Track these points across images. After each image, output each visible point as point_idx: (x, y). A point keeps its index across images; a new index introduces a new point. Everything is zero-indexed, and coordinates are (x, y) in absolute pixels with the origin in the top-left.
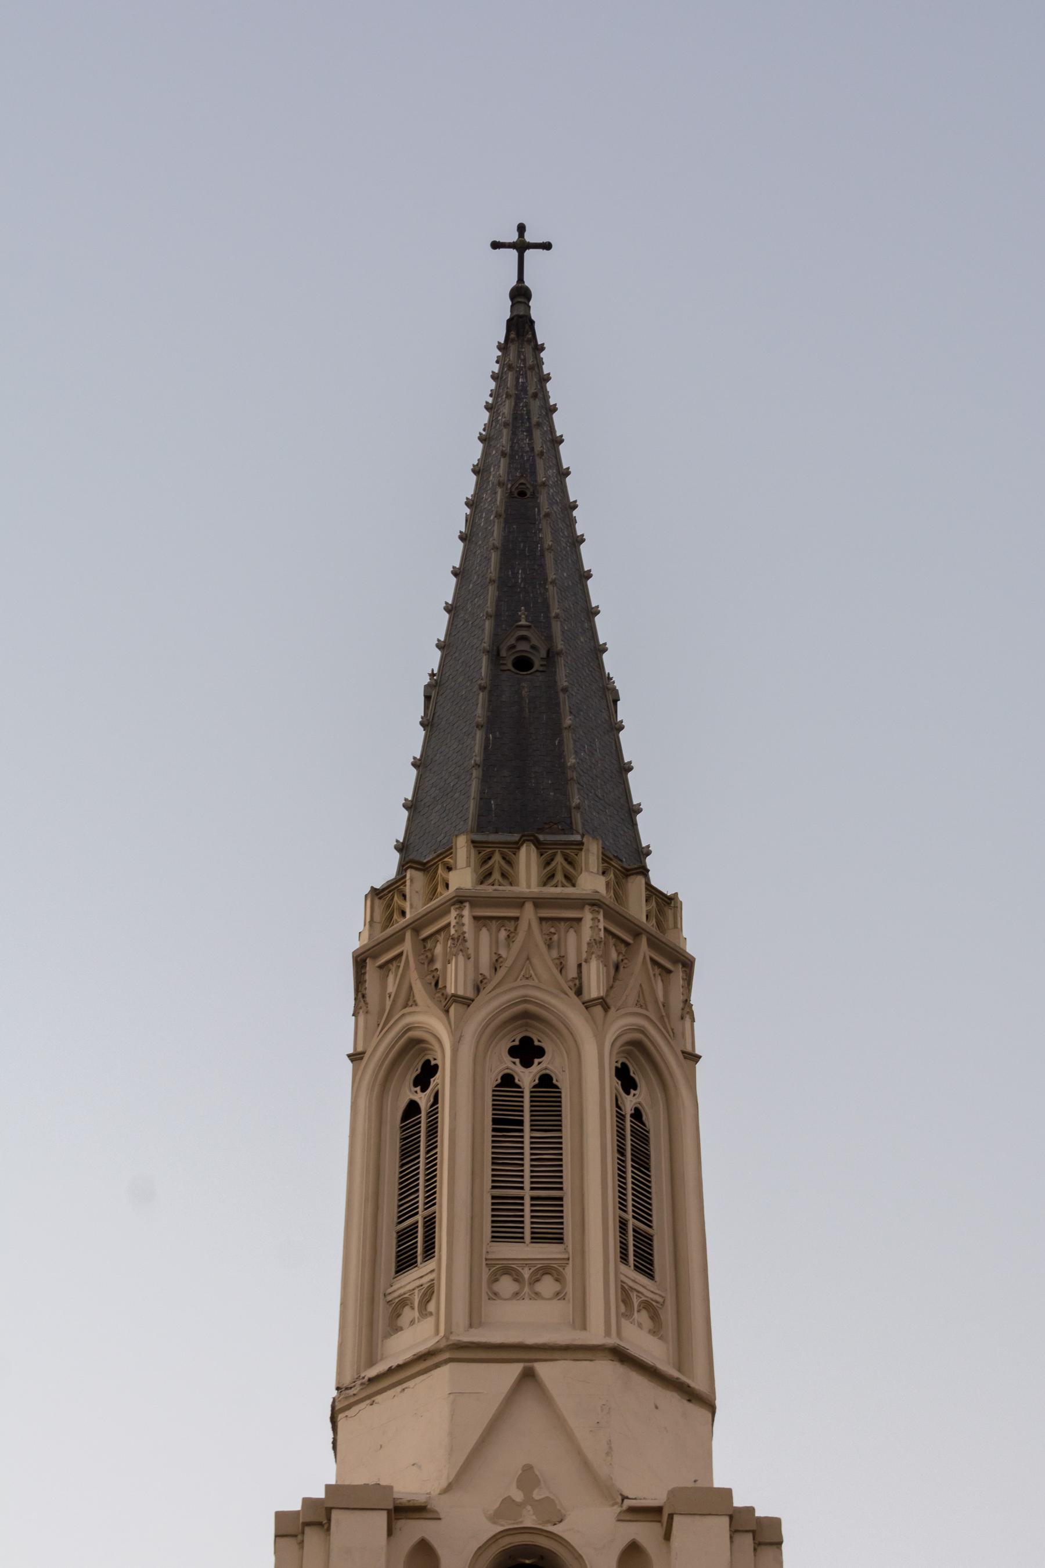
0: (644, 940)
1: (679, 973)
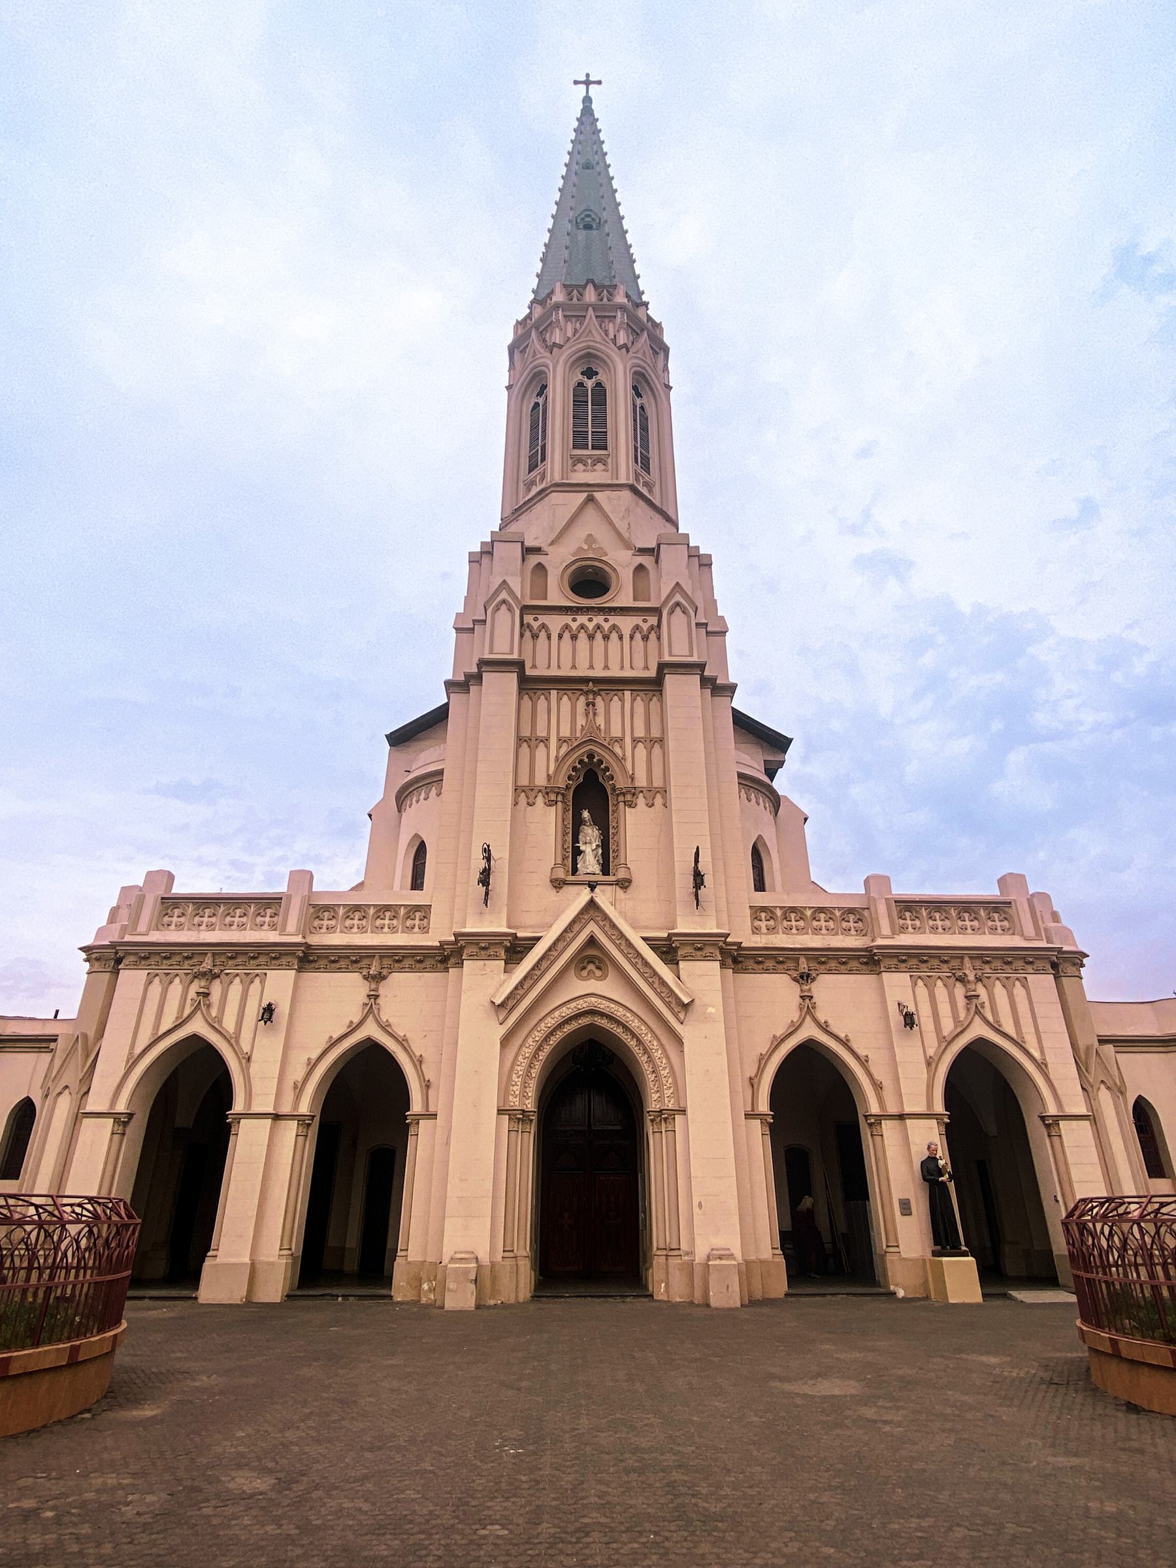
0: (645, 334)
1: (662, 354)
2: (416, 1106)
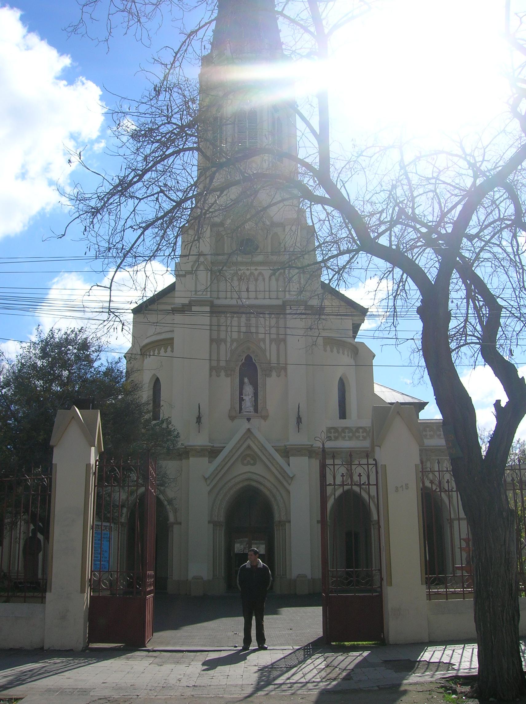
2: (172, 519)
